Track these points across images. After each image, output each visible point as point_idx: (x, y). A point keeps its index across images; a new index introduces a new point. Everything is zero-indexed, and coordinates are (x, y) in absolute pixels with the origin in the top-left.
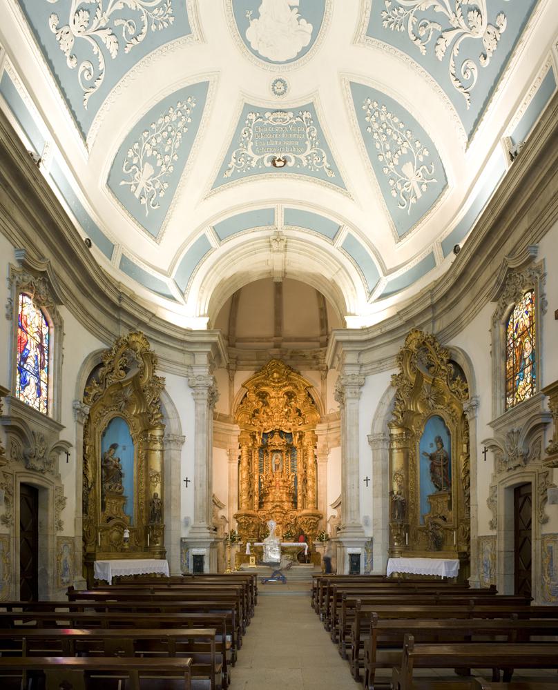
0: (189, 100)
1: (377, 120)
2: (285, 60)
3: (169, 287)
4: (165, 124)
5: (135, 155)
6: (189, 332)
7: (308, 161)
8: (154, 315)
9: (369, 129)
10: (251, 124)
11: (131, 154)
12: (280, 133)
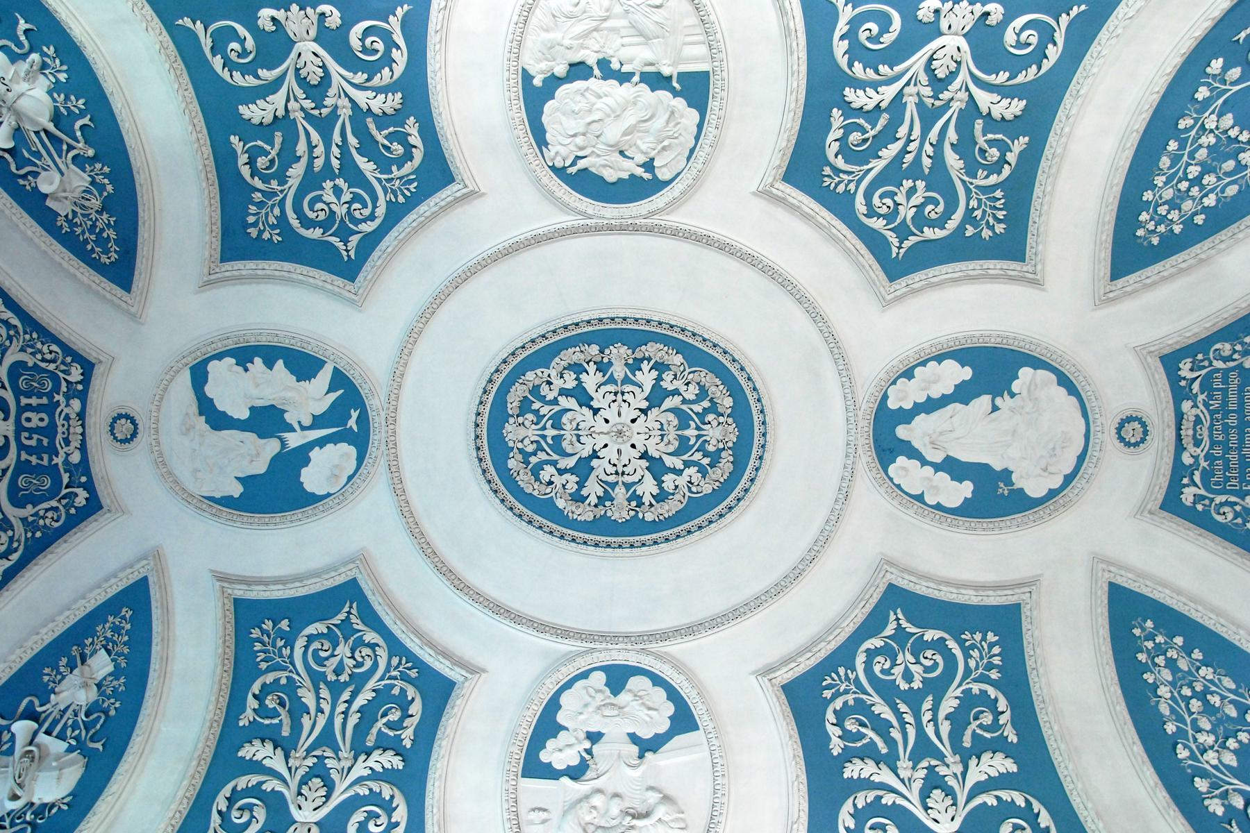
0: (1137, 632)
1: (1174, 205)
9: (1199, 219)
10: (1204, 498)
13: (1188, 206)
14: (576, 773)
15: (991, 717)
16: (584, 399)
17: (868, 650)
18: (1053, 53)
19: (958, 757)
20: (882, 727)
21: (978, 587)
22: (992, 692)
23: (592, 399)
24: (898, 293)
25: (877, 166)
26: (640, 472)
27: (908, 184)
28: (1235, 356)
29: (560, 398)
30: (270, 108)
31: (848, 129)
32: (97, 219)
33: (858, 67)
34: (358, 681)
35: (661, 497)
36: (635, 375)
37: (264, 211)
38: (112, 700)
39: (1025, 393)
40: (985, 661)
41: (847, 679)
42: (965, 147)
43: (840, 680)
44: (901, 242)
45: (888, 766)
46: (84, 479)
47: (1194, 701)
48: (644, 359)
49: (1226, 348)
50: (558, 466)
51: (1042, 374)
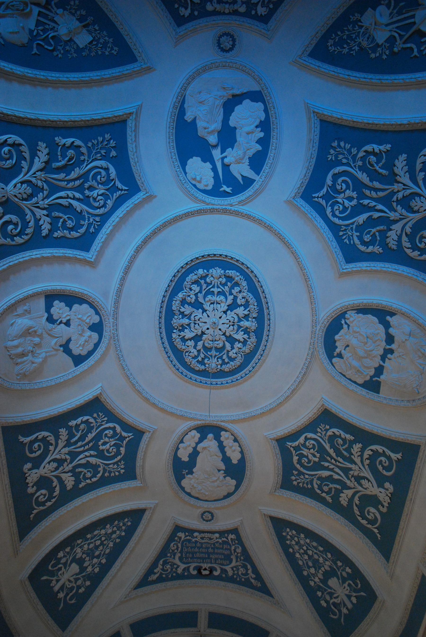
0: (126, 520)
4: (100, 535)
7: (234, 571)
11: (61, 554)
12: (208, 548)
13: (297, 547)
14: (50, 319)
16: (232, 307)
18: (364, 522)
20: (82, 438)
21: (143, 467)
22: (99, 475)
23: (231, 311)
25: (327, 447)
26: (196, 331)
29: (232, 296)
30: (402, 174)
32: (355, 42)
34: (85, 200)
35: (184, 340)
36: (242, 331)
37: (346, 152)
38: (62, 52)
44: (293, 447)
46: (196, 13)
47: (99, 541)
48: (249, 336)
49: (239, 550)
50: (199, 294)
51: (233, 488)
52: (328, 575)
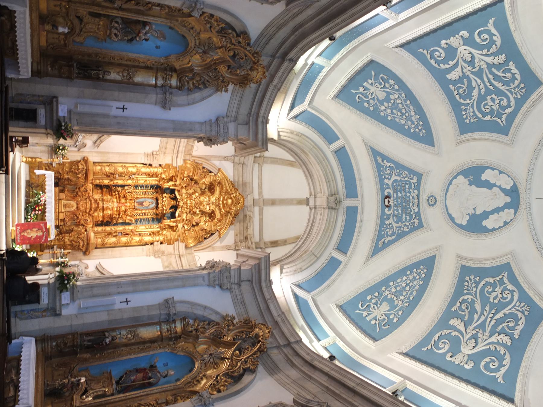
0: (424, 131)
2: (447, 205)
3: (301, 106)
4: (410, 112)
5: (391, 86)
6: (266, 121)
7: (389, 225)
8: (279, 90)
10: (411, 179)
11: (391, 82)
12: (406, 203)
15: (460, 92)
17: (511, 107)
19: (466, 74)
21: (474, 139)
22: (462, 101)
24: (506, 257)
25: (506, 311)
27: (496, 301)
28: (403, 226)
31: (513, 328)
33: (502, 352)
39: (465, 215)
40: (468, 112)
41: (516, 94)
42: (473, 311)
43: (519, 92)
44: (502, 278)
45: (489, 64)
49: (406, 229)
51: (459, 222)
52: (391, 302)
